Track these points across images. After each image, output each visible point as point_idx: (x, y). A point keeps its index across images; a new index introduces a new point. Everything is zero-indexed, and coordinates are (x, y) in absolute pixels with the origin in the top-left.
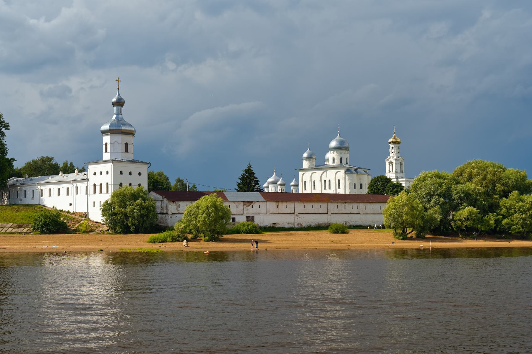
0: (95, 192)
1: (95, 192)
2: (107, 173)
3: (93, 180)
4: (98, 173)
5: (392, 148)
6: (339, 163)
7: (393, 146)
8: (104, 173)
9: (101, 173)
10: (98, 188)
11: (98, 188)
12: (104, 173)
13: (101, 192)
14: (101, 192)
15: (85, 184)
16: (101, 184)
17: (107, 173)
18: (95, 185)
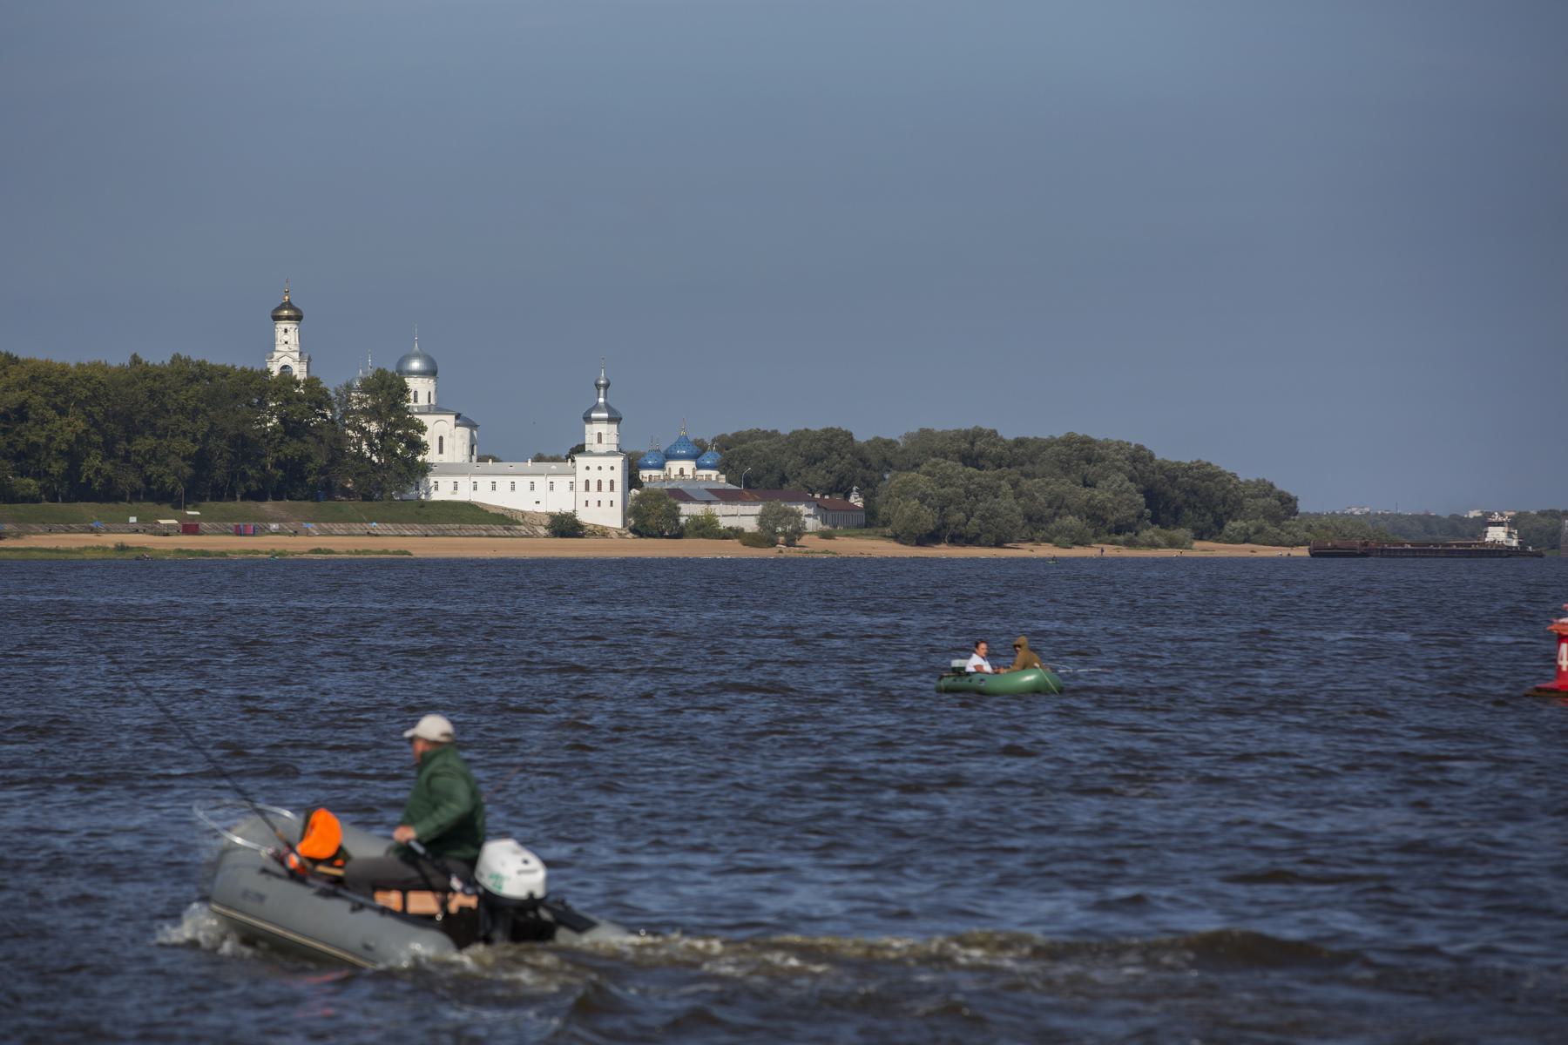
0: (587, 489)
1: (587, 489)
2: (612, 468)
3: (582, 475)
4: (594, 468)
5: (286, 331)
6: (426, 403)
7: (288, 327)
8: (606, 469)
9: (600, 468)
10: (593, 486)
11: (593, 486)
12: (606, 469)
13: (599, 489)
14: (599, 489)
15: (572, 479)
16: (600, 482)
17: (612, 468)
18: (587, 482)
